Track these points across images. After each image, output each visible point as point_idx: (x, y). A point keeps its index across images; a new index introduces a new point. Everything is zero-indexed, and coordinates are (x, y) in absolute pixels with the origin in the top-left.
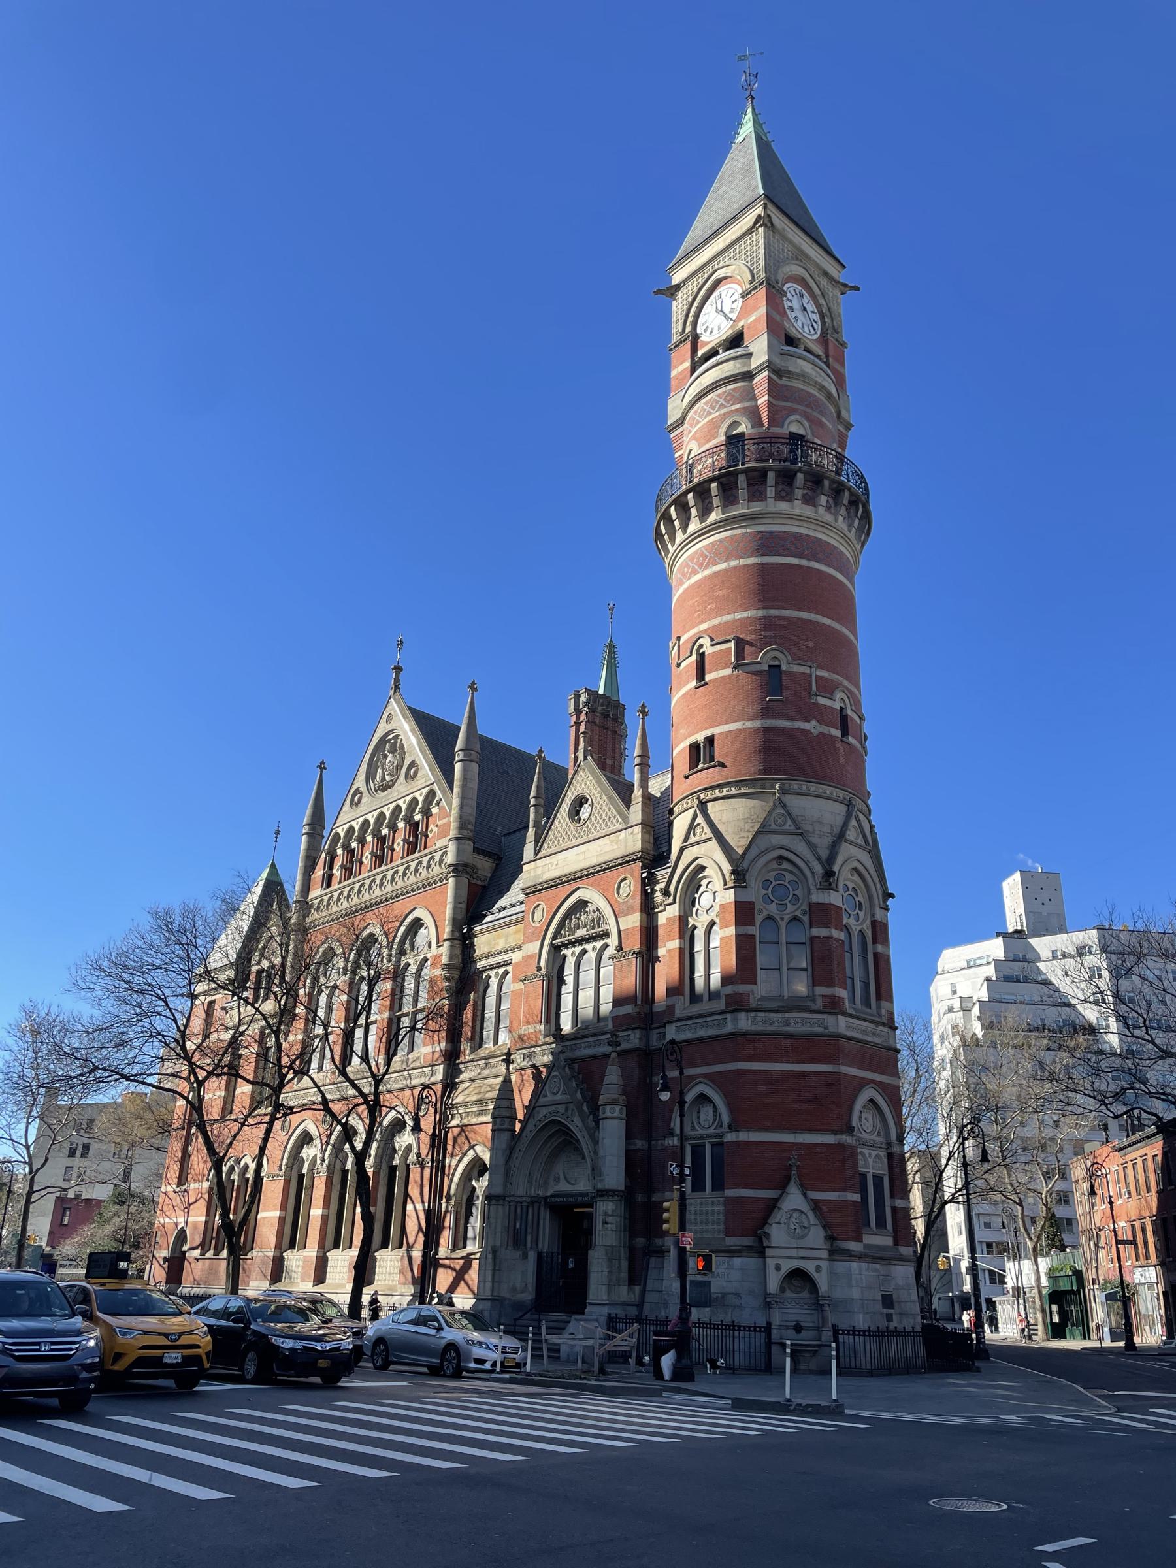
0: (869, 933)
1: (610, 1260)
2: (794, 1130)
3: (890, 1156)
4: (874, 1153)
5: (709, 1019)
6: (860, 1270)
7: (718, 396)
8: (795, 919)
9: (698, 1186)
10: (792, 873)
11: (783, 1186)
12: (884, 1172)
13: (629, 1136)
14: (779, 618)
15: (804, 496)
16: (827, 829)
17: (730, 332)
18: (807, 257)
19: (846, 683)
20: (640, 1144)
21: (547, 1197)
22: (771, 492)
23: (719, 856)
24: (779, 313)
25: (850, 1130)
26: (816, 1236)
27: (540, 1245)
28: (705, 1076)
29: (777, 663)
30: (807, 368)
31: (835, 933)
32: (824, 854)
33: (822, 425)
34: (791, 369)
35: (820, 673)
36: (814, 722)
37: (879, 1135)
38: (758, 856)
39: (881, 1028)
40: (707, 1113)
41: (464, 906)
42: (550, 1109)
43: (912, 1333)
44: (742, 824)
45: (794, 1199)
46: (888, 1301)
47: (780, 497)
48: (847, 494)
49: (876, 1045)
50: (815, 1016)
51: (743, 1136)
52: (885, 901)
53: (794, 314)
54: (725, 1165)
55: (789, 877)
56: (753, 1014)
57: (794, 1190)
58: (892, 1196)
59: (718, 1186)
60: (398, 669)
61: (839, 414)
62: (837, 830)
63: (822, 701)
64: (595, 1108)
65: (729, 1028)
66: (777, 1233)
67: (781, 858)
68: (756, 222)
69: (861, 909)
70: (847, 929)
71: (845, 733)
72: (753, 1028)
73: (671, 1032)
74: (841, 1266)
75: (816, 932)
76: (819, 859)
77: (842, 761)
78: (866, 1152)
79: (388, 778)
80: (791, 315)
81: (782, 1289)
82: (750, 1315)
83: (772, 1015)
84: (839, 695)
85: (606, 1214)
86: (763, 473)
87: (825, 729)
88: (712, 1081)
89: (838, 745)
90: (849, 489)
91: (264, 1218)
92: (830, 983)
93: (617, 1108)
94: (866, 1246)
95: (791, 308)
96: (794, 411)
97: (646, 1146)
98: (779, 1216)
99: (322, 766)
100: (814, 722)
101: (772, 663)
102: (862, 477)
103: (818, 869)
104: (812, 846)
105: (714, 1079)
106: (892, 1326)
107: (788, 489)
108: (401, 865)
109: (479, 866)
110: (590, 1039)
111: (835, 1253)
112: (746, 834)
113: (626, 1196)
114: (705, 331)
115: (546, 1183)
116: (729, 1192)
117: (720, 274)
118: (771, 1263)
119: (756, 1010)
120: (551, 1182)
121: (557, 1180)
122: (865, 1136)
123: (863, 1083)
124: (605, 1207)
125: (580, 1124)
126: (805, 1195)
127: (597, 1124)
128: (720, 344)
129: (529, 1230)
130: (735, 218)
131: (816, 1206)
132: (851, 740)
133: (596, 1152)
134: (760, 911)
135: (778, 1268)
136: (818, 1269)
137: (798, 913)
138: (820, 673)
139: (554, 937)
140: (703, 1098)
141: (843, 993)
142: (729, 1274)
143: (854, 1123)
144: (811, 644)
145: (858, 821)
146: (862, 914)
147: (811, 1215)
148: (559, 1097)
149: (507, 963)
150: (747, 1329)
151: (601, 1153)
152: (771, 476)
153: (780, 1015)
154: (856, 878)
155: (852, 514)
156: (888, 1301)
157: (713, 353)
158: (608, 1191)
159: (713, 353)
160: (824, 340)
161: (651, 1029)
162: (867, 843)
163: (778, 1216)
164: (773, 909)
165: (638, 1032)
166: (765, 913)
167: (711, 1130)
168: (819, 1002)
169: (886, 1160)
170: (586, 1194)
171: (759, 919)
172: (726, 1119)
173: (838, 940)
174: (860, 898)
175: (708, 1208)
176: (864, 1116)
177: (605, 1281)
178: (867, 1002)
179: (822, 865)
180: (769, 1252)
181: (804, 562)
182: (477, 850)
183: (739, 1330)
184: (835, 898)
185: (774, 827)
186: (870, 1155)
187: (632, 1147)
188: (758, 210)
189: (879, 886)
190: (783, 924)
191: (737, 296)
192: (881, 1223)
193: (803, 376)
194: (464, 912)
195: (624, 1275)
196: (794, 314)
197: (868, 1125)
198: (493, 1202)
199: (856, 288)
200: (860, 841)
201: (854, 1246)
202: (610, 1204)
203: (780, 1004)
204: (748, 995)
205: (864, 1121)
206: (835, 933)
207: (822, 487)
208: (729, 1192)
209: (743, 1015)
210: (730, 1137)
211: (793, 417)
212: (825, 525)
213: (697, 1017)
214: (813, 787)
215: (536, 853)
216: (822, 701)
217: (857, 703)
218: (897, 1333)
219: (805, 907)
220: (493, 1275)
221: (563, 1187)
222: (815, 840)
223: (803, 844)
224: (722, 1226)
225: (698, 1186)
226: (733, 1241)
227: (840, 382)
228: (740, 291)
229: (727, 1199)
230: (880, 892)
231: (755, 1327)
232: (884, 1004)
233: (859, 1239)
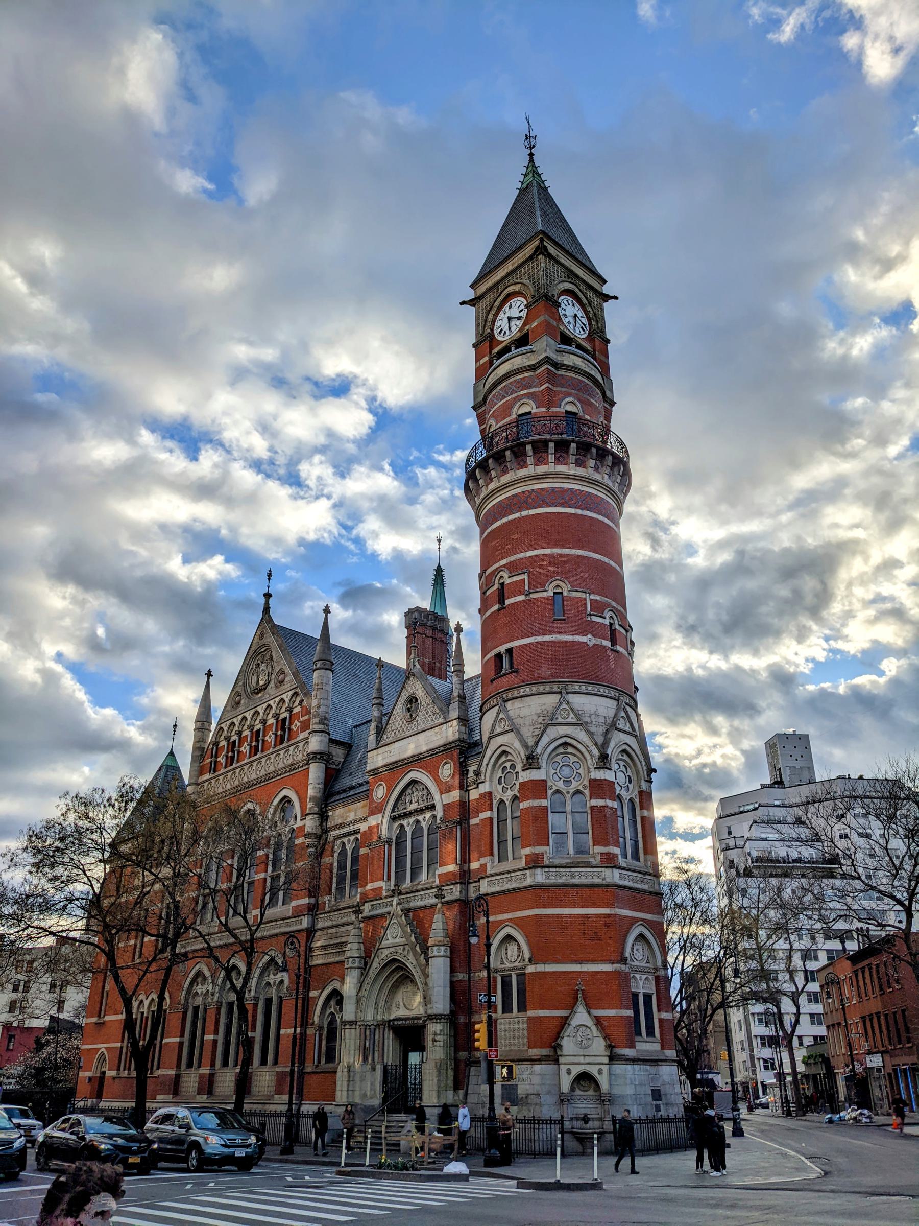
0: (637, 801)
1: (439, 1071)
2: (580, 962)
3: (657, 979)
4: (644, 977)
5: (513, 874)
6: (634, 1070)
7: (510, 383)
8: (578, 792)
9: (507, 1008)
10: (575, 755)
11: (572, 1007)
12: (654, 991)
13: (453, 970)
14: (560, 555)
15: (576, 460)
16: (602, 720)
17: (518, 334)
18: (577, 276)
19: (614, 604)
20: (461, 976)
21: (390, 1021)
22: (551, 458)
23: (517, 745)
24: (555, 319)
25: (624, 960)
26: (599, 1045)
27: (385, 1061)
28: (510, 920)
29: (560, 590)
30: (578, 362)
31: (610, 803)
32: (600, 740)
33: (591, 404)
34: (565, 362)
35: (593, 597)
36: (589, 636)
37: (648, 962)
38: (550, 744)
39: (647, 877)
40: (512, 949)
42: (391, 950)
43: (675, 1120)
44: (535, 718)
45: (581, 1016)
46: (657, 1094)
47: (558, 462)
48: (610, 458)
49: (644, 891)
50: (595, 869)
51: (540, 968)
52: (649, 776)
53: (567, 320)
54: (521, 992)
55: (573, 759)
56: (547, 870)
57: (581, 1009)
58: (659, 1010)
59: (522, 1008)
60: (268, 596)
61: (604, 394)
62: (609, 721)
63: (595, 619)
64: (425, 949)
65: (529, 882)
66: (568, 1045)
67: (566, 744)
68: (536, 251)
69: (630, 782)
70: (619, 798)
71: (614, 642)
72: (547, 881)
73: (485, 887)
74: (619, 1068)
75: (594, 802)
76: (596, 744)
77: (612, 666)
78: (638, 976)
79: (261, 683)
80: (565, 321)
81: (572, 1089)
82: (549, 1111)
83: (561, 870)
84: (608, 614)
85: (435, 1034)
86: (545, 443)
87: (598, 641)
88: (517, 925)
89: (609, 653)
90: (613, 454)
91: (167, 1043)
92: (607, 844)
93: (443, 948)
94: (637, 1051)
95: (565, 315)
96: (569, 395)
97: (466, 978)
98: (569, 1030)
99: (209, 674)
100: (589, 636)
101: (555, 590)
103: (596, 752)
104: (591, 734)
105: (518, 923)
106: (663, 1113)
107: (565, 455)
108: (272, 753)
109: (334, 754)
110: (421, 893)
111: (613, 1058)
112: (539, 726)
113: (451, 1018)
114: (500, 332)
115: (389, 1009)
116: (530, 1013)
117: (511, 289)
118: (563, 1068)
119: (548, 867)
120: (393, 1008)
121: (398, 1007)
122: (636, 963)
123: (634, 921)
124: (434, 1028)
125: (414, 962)
126: (589, 1012)
127: (427, 961)
128: (511, 343)
129: (376, 1048)
130: (520, 248)
131: (598, 1021)
132: (619, 648)
133: (426, 984)
134: (551, 787)
135: (569, 1072)
137: (580, 788)
138: (593, 597)
139: (393, 811)
140: (509, 938)
141: (617, 851)
142: (531, 1079)
143: (627, 954)
144: (586, 575)
145: (626, 713)
146: (631, 786)
147: (594, 1028)
148: (397, 940)
149: (356, 832)
150: (545, 1122)
151: (431, 985)
152: (551, 445)
153: (568, 870)
154: (625, 757)
155: (616, 473)
156: (657, 1094)
157: (507, 350)
158: (436, 1015)
159: (507, 350)
160: (590, 338)
161: (469, 883)
162: (633, 729)
163: (569, 1031)
164: (561, 785)
165: (458, 886)
166: (555, 788)
167: (516, 964)
168: (598, 858)
169: (654, 982)
170: (418, 1018)
171: (550, 792)
172: (527, 955)
173: (612, 808)
174: (629, 773)
175: (513, 1028)
176: (636, 947)
177: (436, 1089)
178: (636, 857)
179: (598, 749)
180: (562, 1060)
181: (579, 512)
182: (331, 741)
183: (538, 1123)
184: (608, 775)
185: (560, 720)
186: (641, 979)
187: (455, 979)
188: (537, 243)
189: (644, 763)
190: (568, 796)
191: (522, 307)
192: (650, 1032)
193: (575, 369)
194: (322, 791)
195: (450, 1082)
196: (567, 320)
197: (639, 955)
198: (347, 1026)
199: (616, 298)
200: (628, 728)
201: (629, 1052)
202: (438, 1025)
203: (569, 861)
204: (542, 855)
205: (636, 954)
206: (610, 803)
207: (591, 453)
208: (530, 1013)
209: (538, 871)
210: (531, 969)
211: (568, 400)
212: (595, 483)
213: (503, 873)
214: (590, 689)
215: (377, 744)
216: (595, 619)
217: (623, 617)
218: (662, 1120)
219: (586, 783)
220: (348, 1085)
221: (402, 1012)
222: (593, 729)
223: (583, 733)
224: (526, 1040)
225: (507, 1008)
226: (535, 1052)
227: (605, 370)
228: (525, 303)
229: (529, 1018)
230: (645, 768)
231: (551, 1121)
232: (649, 857)
233: (632, 1045)
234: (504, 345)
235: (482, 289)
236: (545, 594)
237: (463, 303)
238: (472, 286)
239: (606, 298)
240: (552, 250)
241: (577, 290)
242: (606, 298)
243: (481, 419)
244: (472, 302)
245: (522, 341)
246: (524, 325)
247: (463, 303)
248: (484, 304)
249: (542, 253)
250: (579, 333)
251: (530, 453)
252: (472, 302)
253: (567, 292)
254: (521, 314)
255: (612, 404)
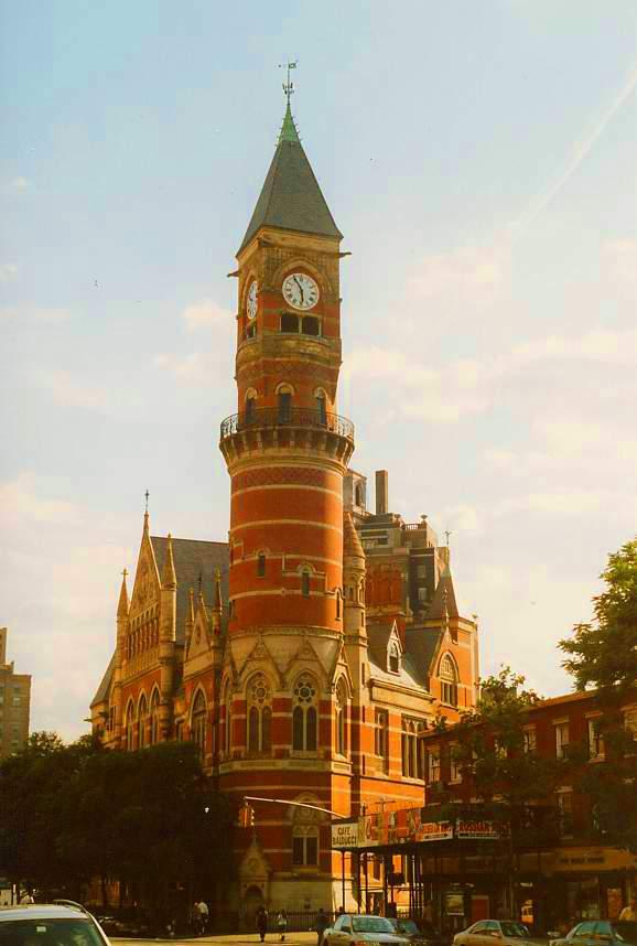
4: (308, 827)
19: (308, 558)
35: (288, 557)
41: (169, 683)
118: (243, 884)
136: (263, 886)
138: (288, 557)
171: (249, 708)
184: (289, 695)
199: (350, 254)
216: (288, 575)
222: (279, 661)
236: (253, 559)
237: (229, 276)
241: (305, 264)
244: (235, 274)
247: (229, 276)
252: (235, 274)
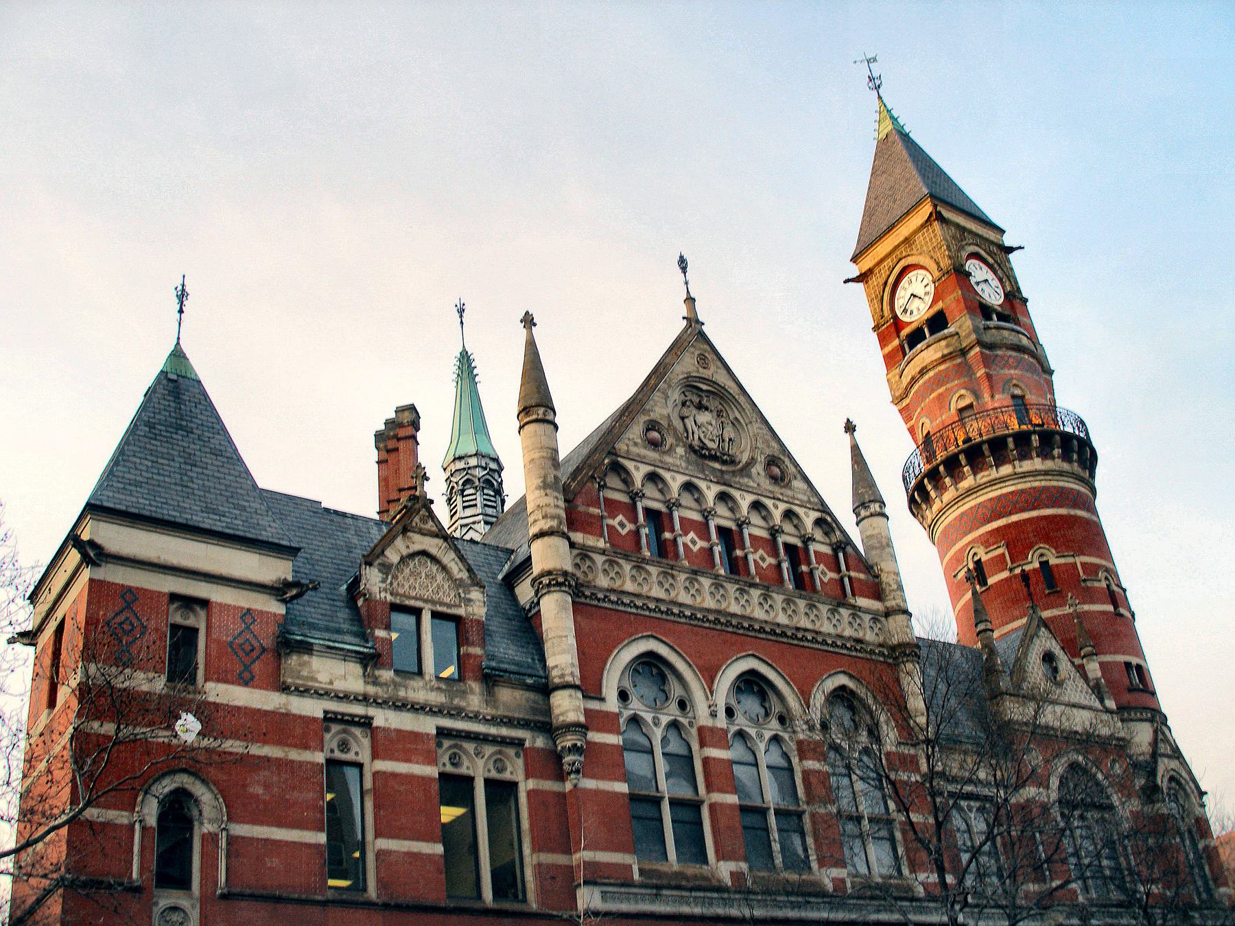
102: (1082, 422)
117: (910, 261)
188: (927, 209)
234: (913, 326)
235: (867, 263)
238: (855, 259)
239: (1010, 250)
240: (947, 214)
242: (1010, 250)
243: (906, 414)
244: (862, 278)
245: (938, 322)
246: (934, 302)
248: (876, 281)
249: (936, 219)
250: (993, 295)
251: (987, 453)
253: (975, 256)
254: (928, 289)
255: (1051, 373)
